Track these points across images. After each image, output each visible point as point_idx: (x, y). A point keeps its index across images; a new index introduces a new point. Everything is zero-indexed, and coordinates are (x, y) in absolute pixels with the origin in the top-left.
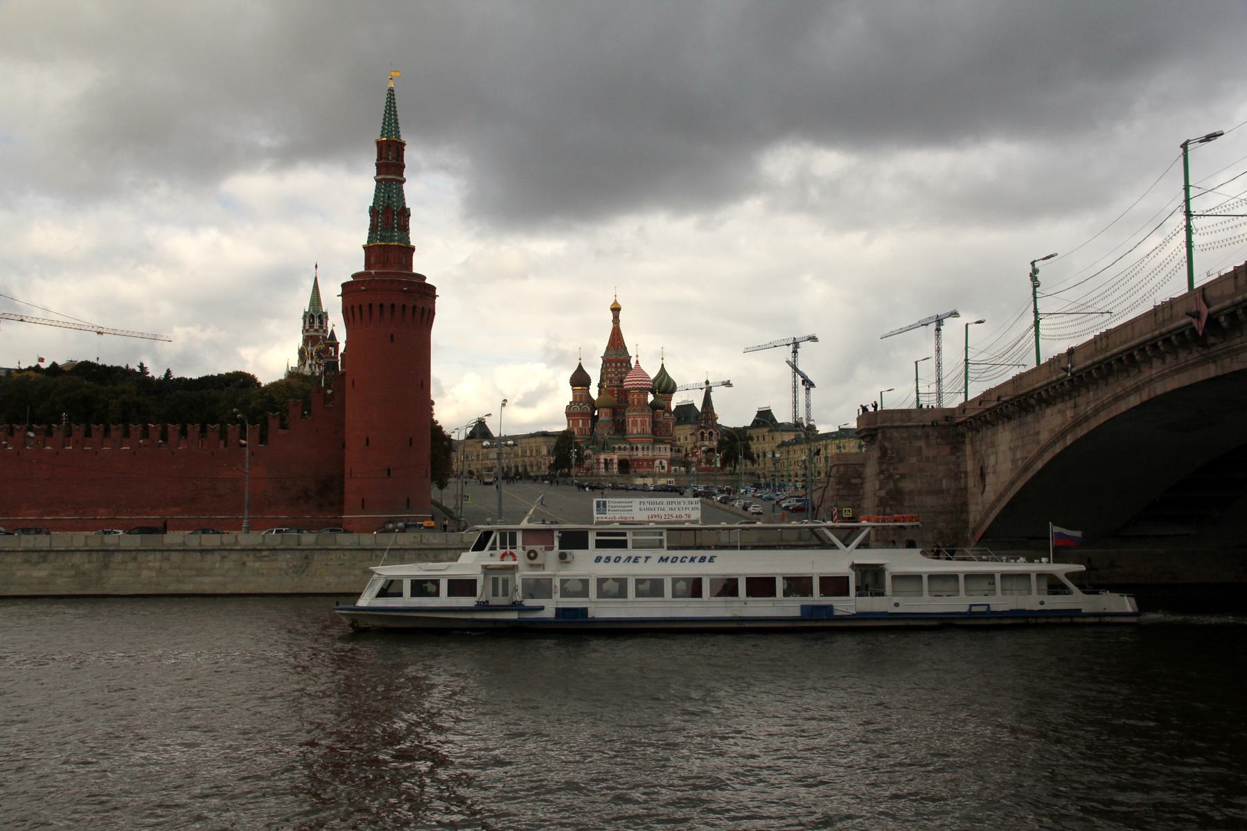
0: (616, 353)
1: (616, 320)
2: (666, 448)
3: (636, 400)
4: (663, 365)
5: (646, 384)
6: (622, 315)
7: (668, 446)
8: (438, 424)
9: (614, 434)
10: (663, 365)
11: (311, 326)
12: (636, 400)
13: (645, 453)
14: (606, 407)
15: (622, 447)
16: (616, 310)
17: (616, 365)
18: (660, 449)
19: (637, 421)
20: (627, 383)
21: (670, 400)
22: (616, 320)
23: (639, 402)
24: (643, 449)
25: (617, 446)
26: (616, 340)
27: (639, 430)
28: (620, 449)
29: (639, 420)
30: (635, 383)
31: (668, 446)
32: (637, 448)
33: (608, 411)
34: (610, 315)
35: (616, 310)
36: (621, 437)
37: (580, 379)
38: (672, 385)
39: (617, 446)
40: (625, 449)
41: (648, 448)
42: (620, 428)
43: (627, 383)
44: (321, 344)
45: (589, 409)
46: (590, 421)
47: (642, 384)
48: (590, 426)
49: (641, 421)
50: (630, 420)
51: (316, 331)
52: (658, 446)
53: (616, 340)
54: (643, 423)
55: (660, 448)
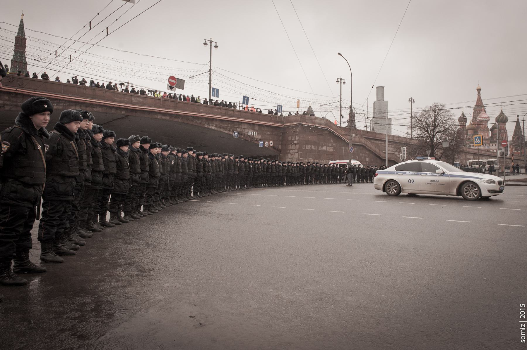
0: (479, 107)
1: (479, 94)
2: (495, 145)
4: (502, 110)
5: (485, 119)
6: (481, 92)
10: (502, 110)
14: (471, 129)
16: (479, 90)
17: (477, 112)
18: (493, 146)
20: (478, 119)
22: (479, 94)
30: (484, 118)
33: (471, 131)
35: (479, 90)
38: (505, 118)
43: (478, 119)
47: (483, 119)
52: (492, 144)
55: (492, 145)
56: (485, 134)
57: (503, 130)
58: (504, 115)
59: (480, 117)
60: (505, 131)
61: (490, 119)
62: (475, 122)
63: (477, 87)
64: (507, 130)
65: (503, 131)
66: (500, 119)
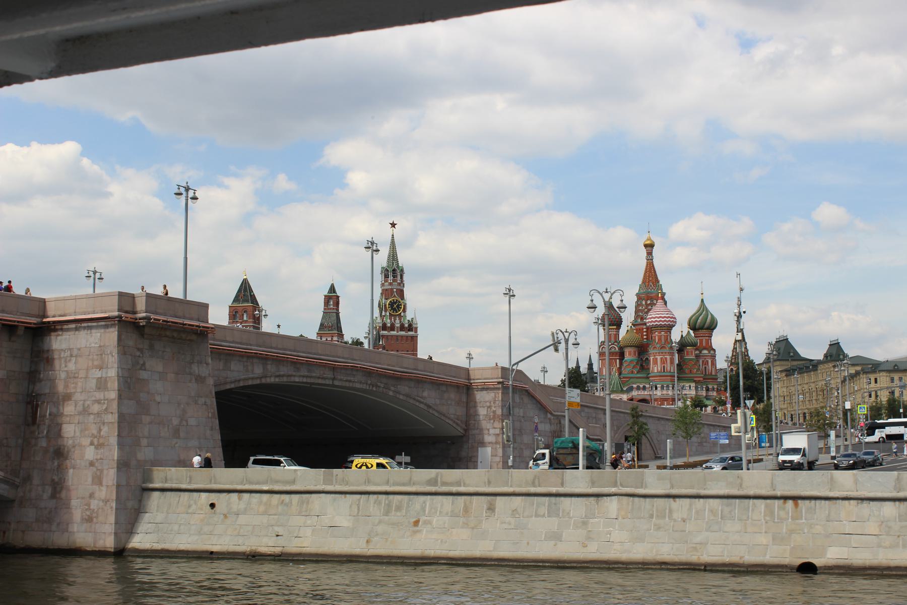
2: (690, 387)
3: (657, 337)
4: (702, 300)
7: (693, 385)
8: (574, 368)
9: (638, 372)
10: (702, 300)
11: (386, 281)
12: (657, 337)
13: (665, 392)
14: (630, 346)
15: (641, 386)
19: (657, 359)
21: (711, 337)
23: (660, 339)
24: (662, 388)
25: (635, 386)
26: (651, 276)
27: (659, 369)
28: (638, 388)
29: (659, 358)
31: (693, 385)
32: (656, 388)
33: (632, 350)
34: (643, 252)
35: (649, 247)
36: (645, 375)
37: (612, 320)
39: (635, 386)
40: (644, 388)
41: (668, 386)
42: (643, 365)
44: (395, 296)
45: (617, 349)
46: (618, 360)
47: (660, 321)
48: (618, 366)
49: (661, 358)
50: (652, 358)
51: (391, 284)
53: (651, 276)
54: (663, 361)
56: (666, 358)
57: (705, 348)
58: (707, 310)
59: (654, 316)
60: (709, 353)
61: (676, 322)
62: (641, 327)
63: (643, 240)
64: (714, 350)
65: (705, 352)
66: (699, 321)
